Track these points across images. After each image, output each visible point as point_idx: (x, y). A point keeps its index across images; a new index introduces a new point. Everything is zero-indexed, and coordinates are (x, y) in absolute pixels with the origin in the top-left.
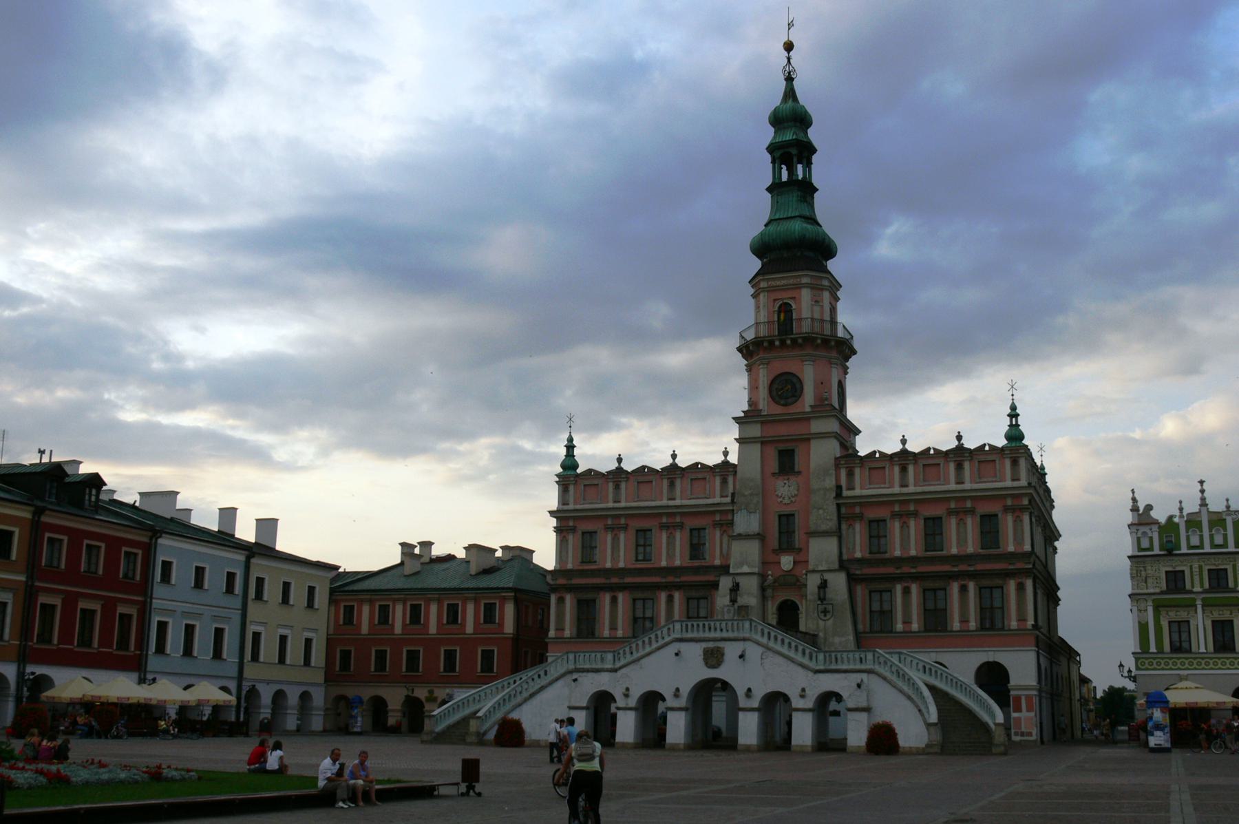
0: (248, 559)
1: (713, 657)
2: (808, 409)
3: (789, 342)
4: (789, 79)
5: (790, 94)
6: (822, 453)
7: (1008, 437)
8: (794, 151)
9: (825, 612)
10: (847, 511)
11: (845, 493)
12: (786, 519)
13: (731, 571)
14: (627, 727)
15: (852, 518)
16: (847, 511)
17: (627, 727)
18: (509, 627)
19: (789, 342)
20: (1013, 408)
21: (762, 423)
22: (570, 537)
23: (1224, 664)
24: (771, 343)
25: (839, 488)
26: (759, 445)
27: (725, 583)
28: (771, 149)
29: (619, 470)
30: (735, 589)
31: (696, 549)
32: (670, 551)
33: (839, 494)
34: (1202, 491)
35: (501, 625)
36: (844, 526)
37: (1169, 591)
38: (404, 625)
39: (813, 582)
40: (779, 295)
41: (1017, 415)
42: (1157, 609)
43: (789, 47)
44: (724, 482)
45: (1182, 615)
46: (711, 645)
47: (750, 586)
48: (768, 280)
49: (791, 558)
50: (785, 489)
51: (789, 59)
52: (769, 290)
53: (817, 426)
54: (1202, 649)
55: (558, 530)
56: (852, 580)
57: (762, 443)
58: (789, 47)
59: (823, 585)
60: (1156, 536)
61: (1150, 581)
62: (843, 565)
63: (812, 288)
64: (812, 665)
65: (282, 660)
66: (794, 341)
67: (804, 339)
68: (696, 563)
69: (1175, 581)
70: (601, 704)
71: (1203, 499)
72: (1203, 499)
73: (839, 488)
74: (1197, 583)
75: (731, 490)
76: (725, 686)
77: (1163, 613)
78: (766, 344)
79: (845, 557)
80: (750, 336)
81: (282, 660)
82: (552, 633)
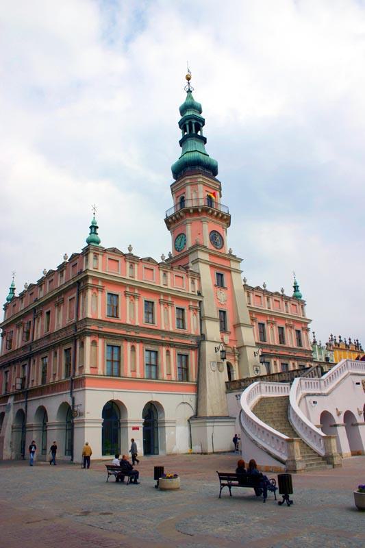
4: (189, 91)
10: (255, 313)
12: (223, 313)
20: (295, 283)
22: (100, 294)
26: (208, 266)
29: (130, 255)
31: (181, 320)
32: (166, 319)
34: (314, 337)
43: (188, 79)
44: (193, 283)
50: (223, 295)
52: (205, 185)
58: (188, 79)
66: (223, 215)
68: (181, 331)
71: (314, 340)
72: (314, 340)
75: (197, 289)
82: (87, 370)
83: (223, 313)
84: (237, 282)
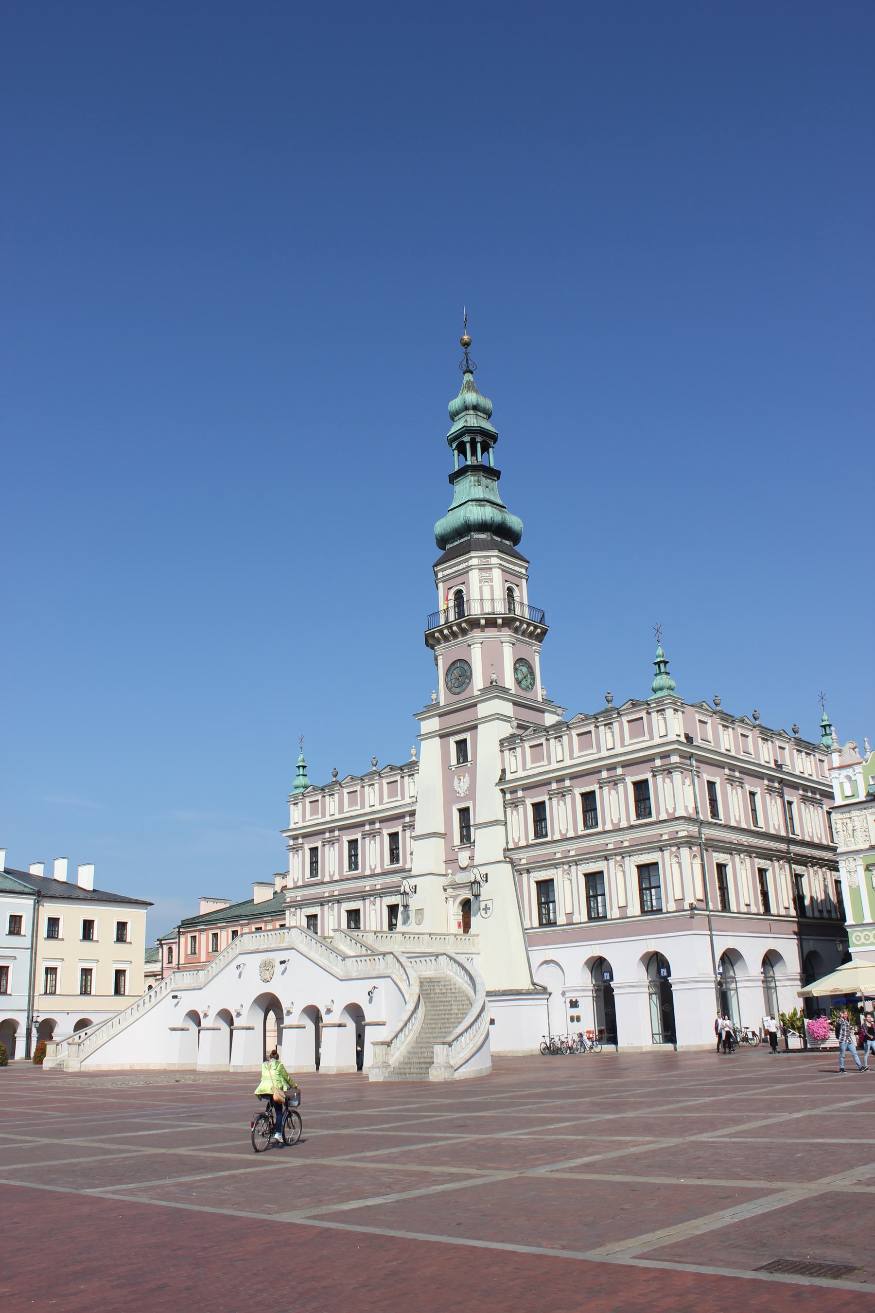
0: (37, 903)
2: (476, 693)
6: (487, 740)
9: (486, 909)
11: (509, 777)
12: (464, 812)
13: (413, 873)
21: (440, 715)
24: (441, 632)
25: (504, 771)
33: (502, 779)
36: (509, 810)
40: (449, 584)
48: (443, 570)
51: (467, 354)
53: (483, 710)
56: (519, 871)
57: (442, 736)
60: (860, 779)
61: (858, 834)
63: (480, 569)
65: (85, 991)
73: (504, 771)
79: (511, 846)
81: (85, 991)
83: (464, 812)
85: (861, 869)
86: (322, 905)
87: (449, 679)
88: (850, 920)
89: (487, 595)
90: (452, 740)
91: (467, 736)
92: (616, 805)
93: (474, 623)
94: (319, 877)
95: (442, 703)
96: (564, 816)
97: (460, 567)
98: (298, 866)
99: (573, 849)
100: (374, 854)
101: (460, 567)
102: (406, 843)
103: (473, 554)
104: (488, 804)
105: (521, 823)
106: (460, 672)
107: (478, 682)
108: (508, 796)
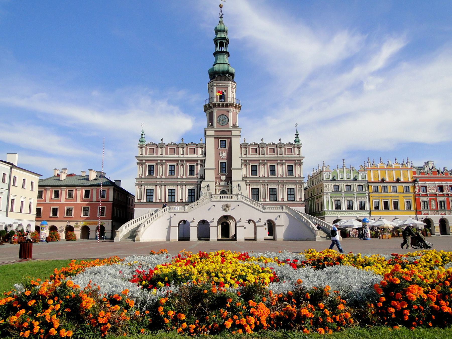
1: (226, 207)
2: (230, 127)
3: (225, 104)
4: (221, 17)
5: (221, 22)
7: (295, 141)
8: (224, 41)
11: (243, 156)
14: (194, 234)
15: (246, 165)
16: (245, 162)
17: (194, 234)
18: (111, 199)
19: (225, 104)
23: (352, 213)
25: (241, 153)
27: (204, 184)
28: (216, 40)
30: (208, 186)
35: (108, 198)
37: (334, 191)
38: (66, 199)
39: (235, 184)
40: (219, 89)
41: (297, 135)
42: (331, 197)
45: (339, 199)
46: (226, 203)
47: (212, 185)
49: (225, 176)
54: (344, 209)
55: (138, 164)
57: (215, 138)
59: (239, 186)
60: (331, 175)
61: (330, 188)
62: (245, 179)
64: (263, 210)
67: (230, 104)
69: (337, 188)
70: (184, 226)
73: (241, 153)
74: (343, 189)
76: (232, 218)
77: (333, 198)
78: (217, 104)
80: (208, 102)
82: (136, 201)
84: (236, 144)
85: (329, 197)
86: (156, 186)
87: (219, 119)
88: (325, 209)
89: (232, 96)
90: (220, 140)
91: (226, 140)
92: (281, 171)
93: (231, 105)
94: (154, 176)
95: (215, 127)
96: (263, 171)
97: (225, 85)
98: (141, 171)
99: (267, 181)
100: (182, 171)
101: (225, 85)
102: (197, 169)
103: (230, 82)
104: (236, 162)
105: (246, 171)
106: (225, 119)
107: (231, 124)
108: (243, 162)
